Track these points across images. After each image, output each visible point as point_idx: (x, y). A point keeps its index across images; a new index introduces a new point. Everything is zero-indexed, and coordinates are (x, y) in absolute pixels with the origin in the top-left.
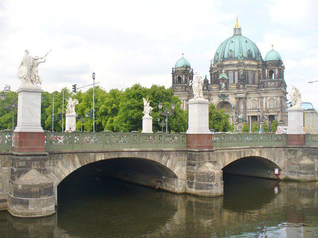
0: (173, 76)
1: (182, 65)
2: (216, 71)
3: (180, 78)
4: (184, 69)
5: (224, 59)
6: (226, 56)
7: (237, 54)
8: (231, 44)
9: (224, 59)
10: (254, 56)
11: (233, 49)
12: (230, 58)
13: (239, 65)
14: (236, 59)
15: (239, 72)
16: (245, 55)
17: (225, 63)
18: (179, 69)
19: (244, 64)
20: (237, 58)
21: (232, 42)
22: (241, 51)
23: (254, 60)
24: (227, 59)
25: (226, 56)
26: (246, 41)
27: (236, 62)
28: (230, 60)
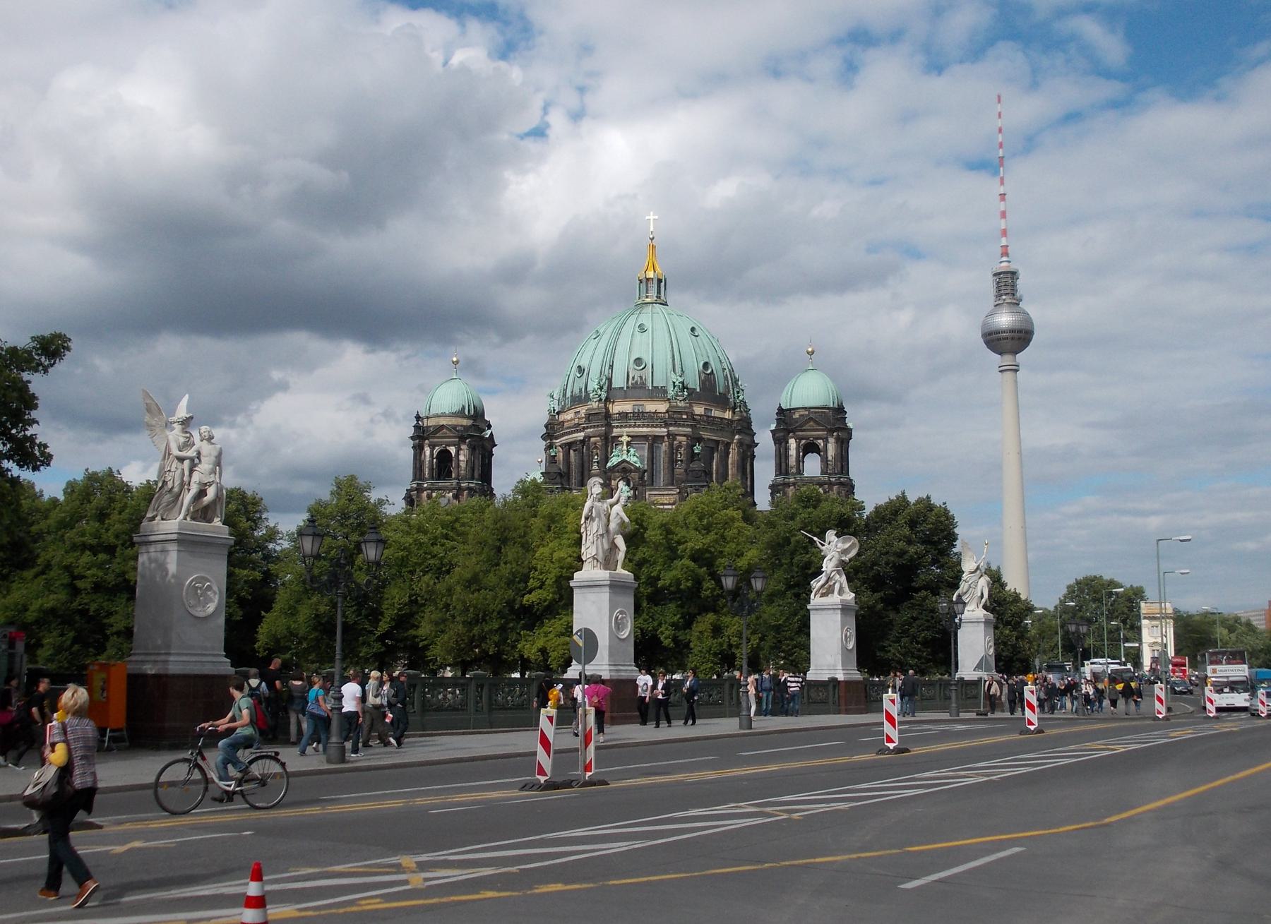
0: (418, 449)
1: (456, 409)
2: (580, 436)
3: (444, 459)
4: (465, 422)
5: (611, 393)
6: (619, 381)
7: (663, 376)
8: (637, 333)
9: (611, 393)
10: (720, 388)
11: (647, 359)
12: (637, 389)
13: (672, 418)
14: (659, 393)
15: (671, 445)
16: (694, 382)
17: (616, 408)
18: (443, 422)
19: (692, 416)
20: (664, 390)
21: (642, 329)
22: (676, 364)
23: (722, 401)
24: (625, 394)
25: (619, 381)
26: (693, 329)
27: (662, 407)
28: (638, 398)
